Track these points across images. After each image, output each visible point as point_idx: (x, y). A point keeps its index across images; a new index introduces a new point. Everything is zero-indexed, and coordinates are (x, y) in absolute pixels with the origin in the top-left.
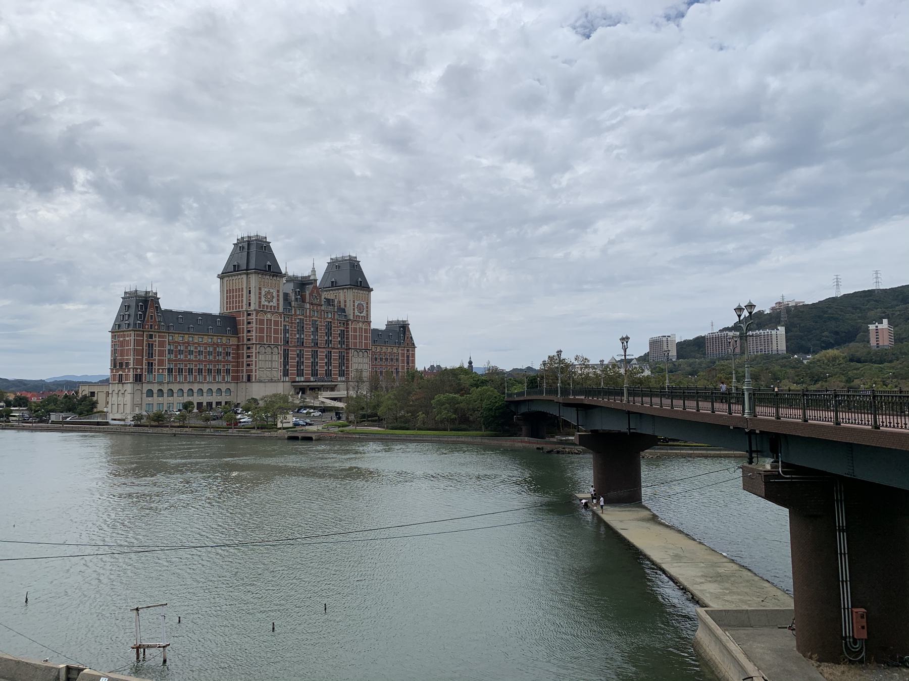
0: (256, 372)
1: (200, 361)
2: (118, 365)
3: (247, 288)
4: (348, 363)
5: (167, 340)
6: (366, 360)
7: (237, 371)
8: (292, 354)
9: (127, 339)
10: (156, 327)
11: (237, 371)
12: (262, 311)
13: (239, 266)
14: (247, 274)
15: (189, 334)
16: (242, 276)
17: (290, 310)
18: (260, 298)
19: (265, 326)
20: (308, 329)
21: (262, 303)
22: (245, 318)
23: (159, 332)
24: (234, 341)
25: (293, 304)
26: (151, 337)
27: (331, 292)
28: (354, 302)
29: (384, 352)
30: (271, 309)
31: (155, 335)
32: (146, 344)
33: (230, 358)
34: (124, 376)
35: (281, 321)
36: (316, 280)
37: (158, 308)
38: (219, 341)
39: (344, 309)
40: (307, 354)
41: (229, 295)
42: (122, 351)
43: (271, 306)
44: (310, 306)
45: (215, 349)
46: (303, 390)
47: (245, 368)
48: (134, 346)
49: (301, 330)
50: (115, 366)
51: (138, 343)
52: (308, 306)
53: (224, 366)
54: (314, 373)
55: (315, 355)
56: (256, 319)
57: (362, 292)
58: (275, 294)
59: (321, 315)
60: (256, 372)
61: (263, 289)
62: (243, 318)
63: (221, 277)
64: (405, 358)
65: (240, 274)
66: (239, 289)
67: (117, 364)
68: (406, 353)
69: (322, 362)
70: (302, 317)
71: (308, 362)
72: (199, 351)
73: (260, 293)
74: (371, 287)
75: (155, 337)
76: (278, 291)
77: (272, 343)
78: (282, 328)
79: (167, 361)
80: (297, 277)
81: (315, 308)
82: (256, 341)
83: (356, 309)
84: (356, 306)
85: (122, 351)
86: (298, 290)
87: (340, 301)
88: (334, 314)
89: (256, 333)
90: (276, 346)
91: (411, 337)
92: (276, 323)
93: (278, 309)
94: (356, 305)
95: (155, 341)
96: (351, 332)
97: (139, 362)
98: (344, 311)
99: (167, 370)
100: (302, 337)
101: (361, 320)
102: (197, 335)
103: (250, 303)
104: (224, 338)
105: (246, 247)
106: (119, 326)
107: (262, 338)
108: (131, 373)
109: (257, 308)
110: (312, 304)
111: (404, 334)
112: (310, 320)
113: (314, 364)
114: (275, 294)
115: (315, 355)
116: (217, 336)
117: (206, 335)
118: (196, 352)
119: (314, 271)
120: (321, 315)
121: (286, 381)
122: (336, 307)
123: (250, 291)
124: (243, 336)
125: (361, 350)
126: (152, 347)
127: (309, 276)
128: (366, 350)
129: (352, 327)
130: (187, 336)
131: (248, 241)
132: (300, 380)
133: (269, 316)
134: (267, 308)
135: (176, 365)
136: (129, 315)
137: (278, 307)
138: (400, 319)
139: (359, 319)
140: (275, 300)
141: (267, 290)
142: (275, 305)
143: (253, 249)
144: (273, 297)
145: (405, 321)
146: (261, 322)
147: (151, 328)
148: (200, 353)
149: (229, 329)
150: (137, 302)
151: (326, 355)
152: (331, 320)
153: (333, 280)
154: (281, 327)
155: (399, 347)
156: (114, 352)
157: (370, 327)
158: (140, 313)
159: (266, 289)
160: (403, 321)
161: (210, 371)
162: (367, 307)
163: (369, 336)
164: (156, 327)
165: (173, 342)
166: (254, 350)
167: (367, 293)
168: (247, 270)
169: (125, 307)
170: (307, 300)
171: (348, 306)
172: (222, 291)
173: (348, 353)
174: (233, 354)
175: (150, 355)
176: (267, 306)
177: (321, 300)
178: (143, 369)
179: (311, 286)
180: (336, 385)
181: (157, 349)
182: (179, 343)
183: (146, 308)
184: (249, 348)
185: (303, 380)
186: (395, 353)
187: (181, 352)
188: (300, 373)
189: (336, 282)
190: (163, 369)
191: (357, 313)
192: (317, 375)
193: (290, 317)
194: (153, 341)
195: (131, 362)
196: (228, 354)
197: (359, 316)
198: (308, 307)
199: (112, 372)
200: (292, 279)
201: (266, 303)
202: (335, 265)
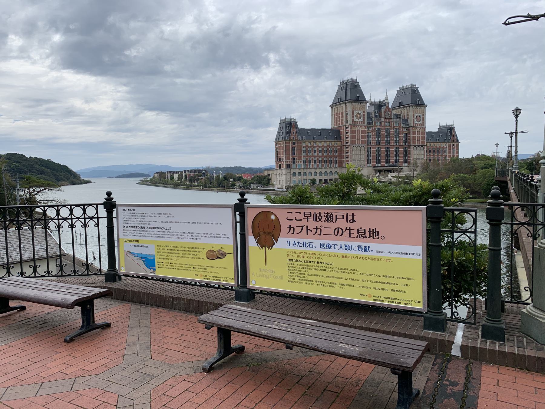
1: (320, 156)
2: (278, 159)
3: (345, 112)
4: (410, 155)
5: (302, 145)
6: (422, 152)
7: (341, 161)
8: (373, 150)
9: (282, 145)
10: (296, 138)
11: (341, 161)
13: (341, 99)
14: (346, 103)
17: (371, 123)
18: (353, 117)
19: (356, 134)
20: (384, 134)
21: (354, 120)
22: (344, 130)
23: (298, 141)
24: (338, 144)
25: (373, 119)
26: (294, 144)
27: (399, 109)
28: (414, 115)
29: (436, 147)
30: (360, 123)
31: (296, 143)
33: (337, 154)
34: (281, 165)
35: (366, 130)
36: (388, 103)
37: (297, 127)
38: (330, 144)
40: (383, 149)
41: (336, 117)
42: (280, 152)
43: (360, 122)
45: (328, 149)
46: (380, 171)
47: (345, 160)
49: (379, 135)
50: (277, 160)
51: (287, 147)
52: (383, 120)
53: (328, 159)
54: (388, 161)
55: (388, 150)
57: (419, 108)
58: (362, 114)
59: (391, 125)
61: (354, 111)
63: (332, 106)
64: (452, 150)
65: (342, 104)
66: (341, 113)
67: (279, 159)
68: (452, 147)
69: (392, 154)
70: (379, 127)
71: (383, 154)
72: (319, 151)
73: (353, 114)
74: (426, 104)
76: (364, 112)
78: (367, 134)
80: (377, 102)
81: (388, 120)
83: (415, 120)
84: (415, 117)
85: (280, 152)
87: (404, 115)
88: (400, 124)
89: (351, 138)
90: (363, 146)
91: (456, 136)
92: (363, 132)
93: (364, 123)
94: (415, 116)
95: (296, 146)
97: (288, 158)
98: (407, 121)
100: (379, 139)
102: (307, 141)
103: (347, 121)
104: (333, 142)
105: (345, 87)
106: (278, 138)
107: (354, 141)
108: (285, 164)
109: (351, 124)
110: (386, 118)
111: (451, 134)
112: (384, 129)
113: (387, 156)
114: (362, 114)
115: (388, 150)
117: (323, 141)
118: (318, 151)
119: (387, 97)
120: (391, 125)
122: (402, 119)
123: (347, 113)
125: (419, 146)
127: (384, 101)
128: (422, 146)
131: (346, 83)
133: (358, 128)
134: (357, 123)
135: (307, 159)
136: (282, 133)
137: (364, 122)
138: (448, 124)
139: (417, 125)
140: (362, 118)
141: (357, 112)
142: (362, 120)
143: (349, 87)
145: (452, 125)
146: (354, 132)
147: (294, 139)
148: (320, 151)
149: (336, 137)
150: (286, 125)
151: (395, 150)
152: (398, 128)
153: (400, 101)
154: (366, 134)
155: (447, 143)
156: (277, 154)
157: (425, 130)
158: (288, 131)
159: (357, 112)
160: (450, 125)
161: (325, 162)
162: (423, 118)
164: (296, 138)
165: (305, 146)
166: (349, 149)
167: (423, 108)
168: (345, 101)
169: (281, 128)
170: (383, 116)
171: (410, 118)
172: (332, 115)
173: (409, 148)
174: (338, 151)
175: (294, 154)
176: (357, 122)
177: (391, 116)
179: (385, 107)
180: (402, 169)
181: (297, 150)
182: (308, 146)
183: (291, 128)
184: (347, 148)
185: (380, 165)
186: (443, 147)
187: (310, 151)
188: (378, 161)
189: (402, 103)
190: (300, 161)
191: (416, 122)
192: (389, 163)
193: (372, 127)
194: (295, 146)
195: (284, 157)
196: (335, 151)
197: (417, 124)
198: (383, 120)
199: (276, 163)
200: (372, 104)
201: (357, 120)
202: (402, 92)
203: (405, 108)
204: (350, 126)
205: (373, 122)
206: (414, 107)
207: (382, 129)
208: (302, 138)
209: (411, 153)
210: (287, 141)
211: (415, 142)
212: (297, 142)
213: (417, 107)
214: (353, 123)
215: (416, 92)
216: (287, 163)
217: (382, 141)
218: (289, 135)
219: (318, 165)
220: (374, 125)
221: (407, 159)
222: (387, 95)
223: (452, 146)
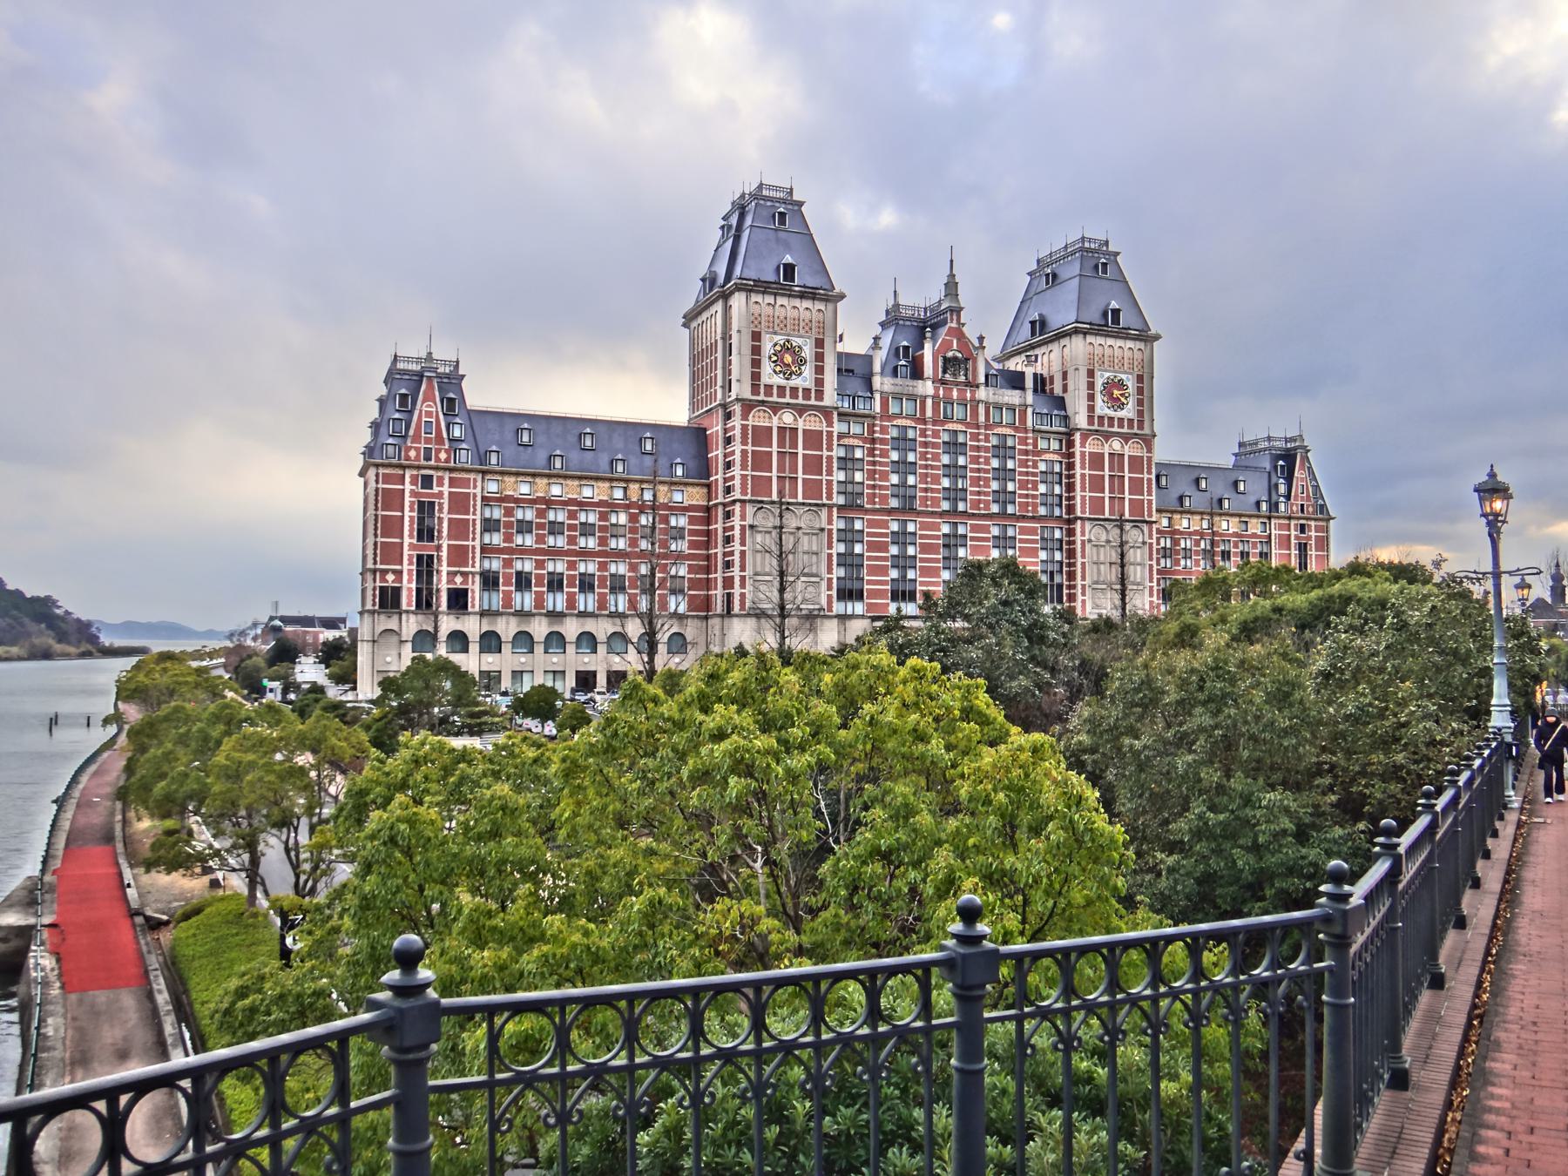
0: (743, 585)
4: (1074, 565)
5: (479, 491)
12: (763, 402)
15: (549, 476)
16: (712, 310)
18: (756, 363)
19: (775, 448)
23: (451, 470)
24: (693, 496)
26: (427, 482)
28: (1091, 373)
32: (412, 503)
33: (681, 546)
36: (957, 311)
39: (1063, 398)
44: (936, 389)
48: (376, 509)
56: (744, 428)
58: (808, 352)
60: (743, 585)
62: (715, 429)
68: (1297, 537)
73: (756, 350)
75: (440, 484)
76: (819, 343)
77: (800, 499)
79: (478, 550)
81: (955, 394)
82: (744, 492)
84: (1099, 387)
86: (905, 343)
92: (813, 438)
93: (820, 395)
95: (440, 495)
96: (1083, 467)
98: (1060, 403)
99: (477, 578)
101: (1115, 429)
107: (761, 485)
109: (747, 394)
110: (943, 382)
114: (808, 352)
116: (642, 482)
118: (572, 528)
119: (951, 287)
121: (853, 617)
124: (717, 480)
126: (432, 515)
129: (1083, 454)
130: (545, 481)
132: (849, 612)
139: (1111, 425)
141: (780, 339)
144: (803, 362)
146: (762, 435)
147: (428, 458)
157: (1150, 450)
159: (777, 338)
163: (1149, 480)
164: (443, 456)
166: (736, 521)
167: (1140, 345)
170: (928, 369)
171: (1071, 387)
173: (1071, 533)
174: (692, 533)
175: (426, 533)
176: (781, 389)
178: (401, 572)
181: (445, 516)
182: (517, 501)
184: (728, 515)
186: (1254, 535)
190: (464, 574)
194: (433, 495)
197: (1111, 419)
201: (778, 380)
203: (1055, 347)
204: (737, 408)
205: (877, 396)
206: (1090, 339)
208: (483, 458)
209: (1079, 554)
210: (384, 465)
211: (1097, 505)
212: (447, 476)
213: (1110, 341)
214: (755, 389)
215: (1105, 272)
216: (383, 580)
217: (926, 490)
218: (405, 437)
219: (507, 595)
220: (878, 409)
221: (1060, 586)
222: (952, 276)
223: (1293, 533)
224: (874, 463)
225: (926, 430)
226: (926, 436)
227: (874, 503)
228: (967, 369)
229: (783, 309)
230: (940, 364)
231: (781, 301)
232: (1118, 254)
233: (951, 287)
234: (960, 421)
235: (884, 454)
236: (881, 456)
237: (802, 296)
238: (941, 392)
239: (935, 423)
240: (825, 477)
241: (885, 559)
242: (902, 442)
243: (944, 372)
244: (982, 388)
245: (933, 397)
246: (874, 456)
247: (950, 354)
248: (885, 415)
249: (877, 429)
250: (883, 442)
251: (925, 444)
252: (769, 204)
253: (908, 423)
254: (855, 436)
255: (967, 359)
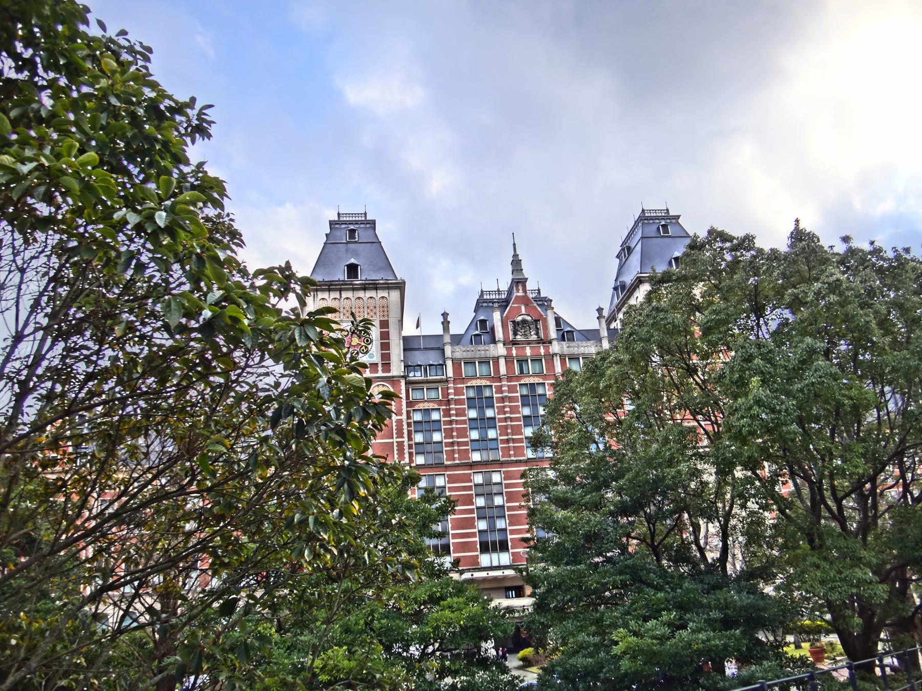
93: (387, 366)
170: (499, 334)
205: (449, 363)
207: (499, 390)
220: (450, 373)
222: (515, 255)
224: (451, 422)
225: (501, 386)
226: (502, 392)
227: (454, 459)
228: (537, 329)
229: (347, 301)
230: (510, 327)
231: (345, 295)
232: (678, 217)
233: (516, 263)
234: (535, 375)
235: (460, 413)
236: (457, 415)
237: (365, 287)
238: (514, 352)
239: (509, 379)
240: (395, 440)
241: (471, 511)
242: (480, 401)
243: (515, 334)
244: (555, 343)
245: (506, 357)
246: (450, 416)
247: (520, 318)
248: (458, 378)
249: (451, 391)
250: (457, 402)
251: (502, 400)
252: (343, 226)
253: (484, 382)
254: (429, 401)
255: (536, 321)
